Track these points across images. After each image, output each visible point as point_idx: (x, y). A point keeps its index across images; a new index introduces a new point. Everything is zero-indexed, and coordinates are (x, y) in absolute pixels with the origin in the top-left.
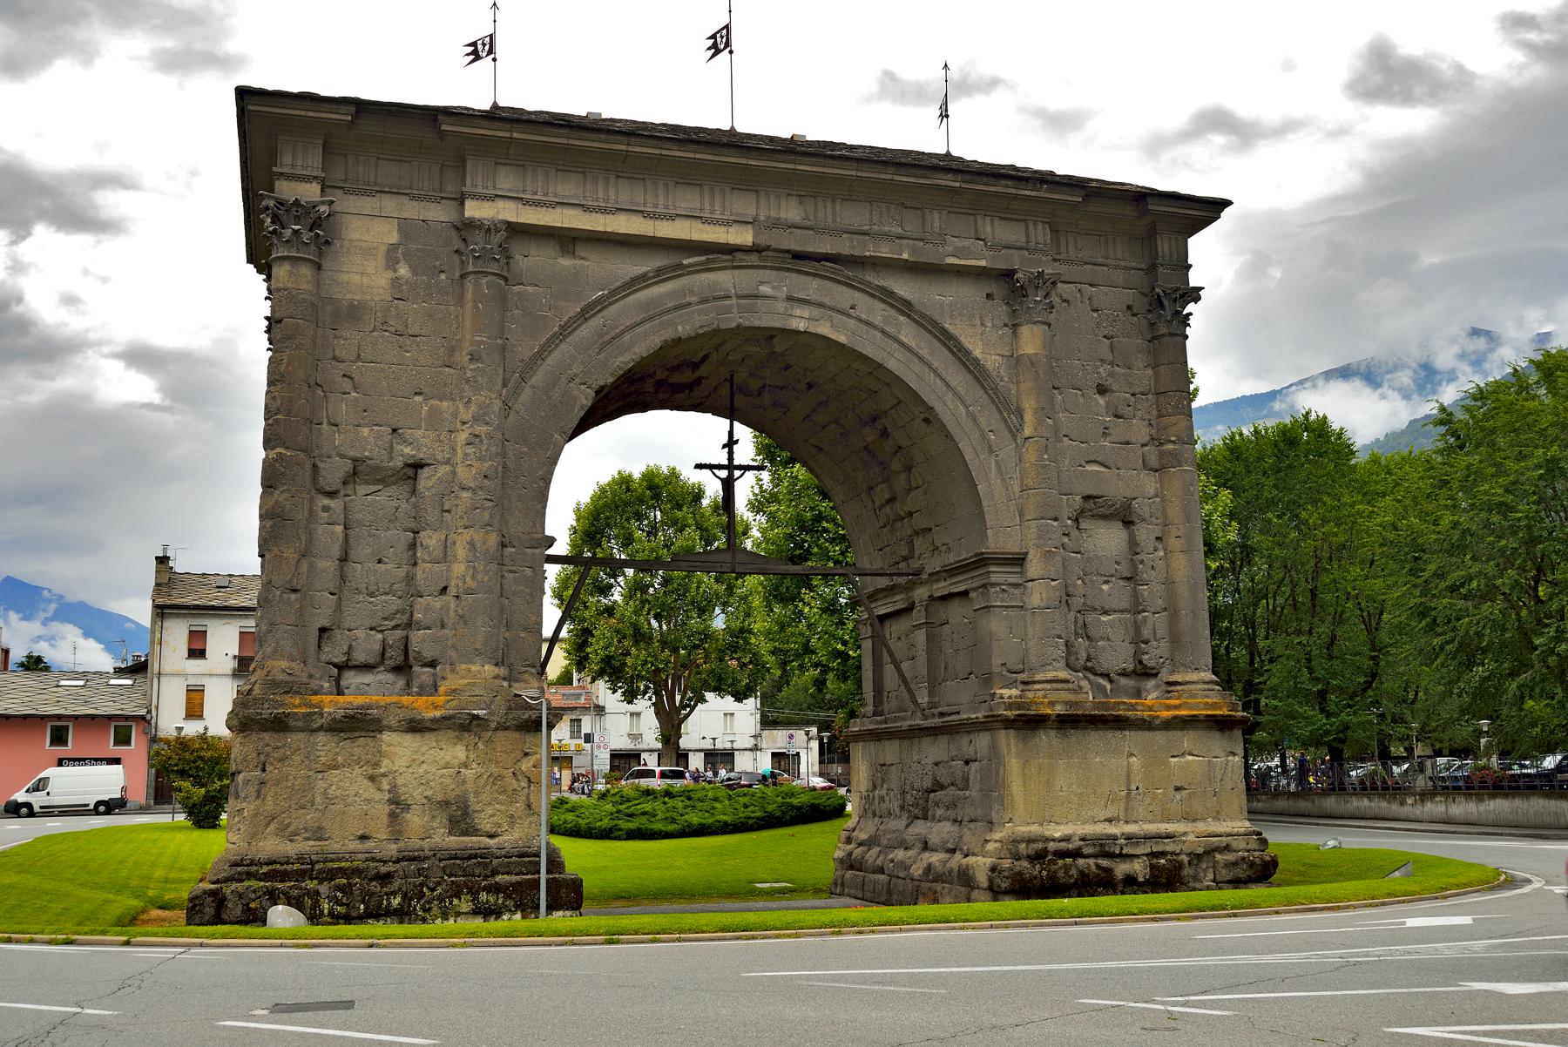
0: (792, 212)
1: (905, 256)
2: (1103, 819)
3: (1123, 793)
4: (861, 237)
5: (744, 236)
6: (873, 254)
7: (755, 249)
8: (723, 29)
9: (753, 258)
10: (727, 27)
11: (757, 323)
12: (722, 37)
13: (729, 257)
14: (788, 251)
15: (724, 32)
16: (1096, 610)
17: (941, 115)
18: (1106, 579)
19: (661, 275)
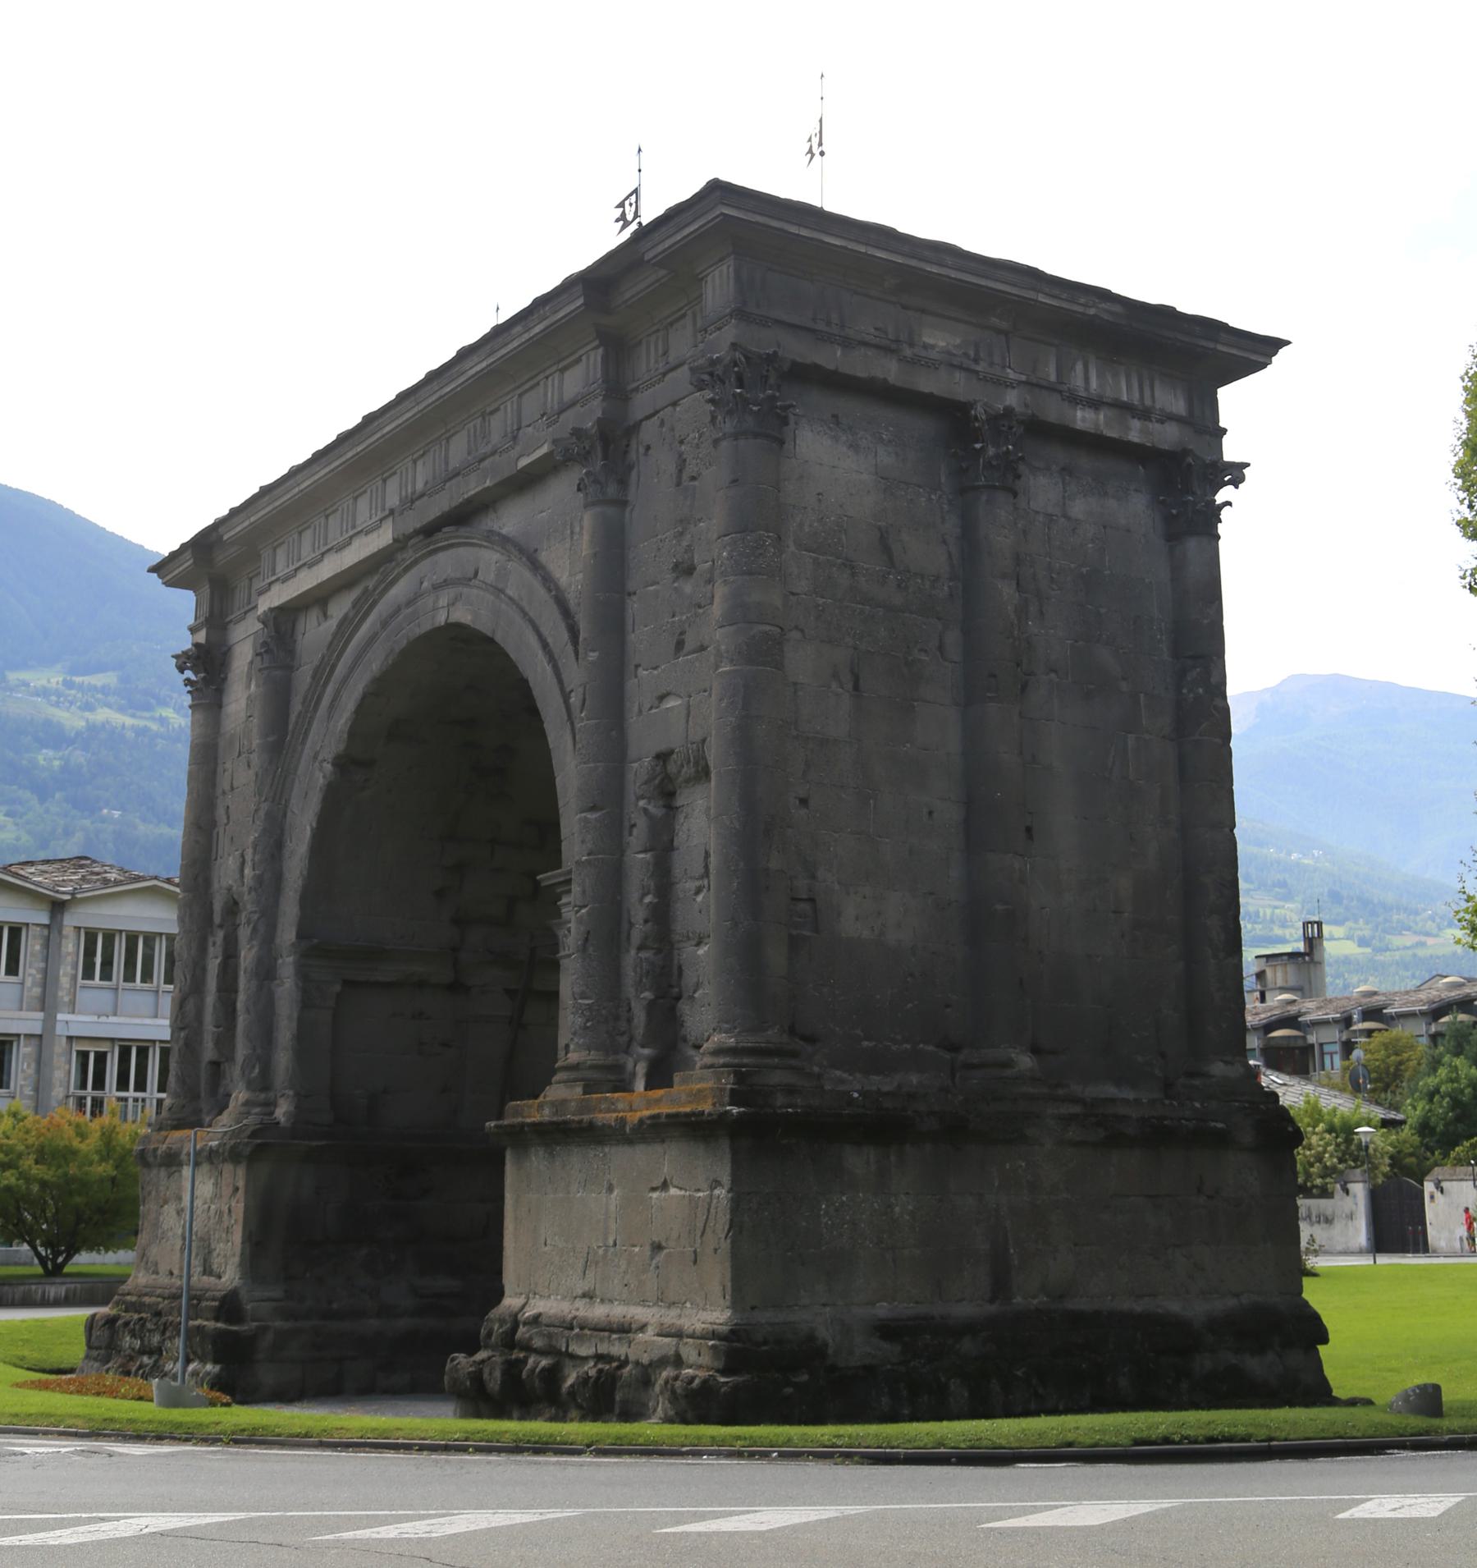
0: (421, 475)
1: (488, 483)
2: (580, 1292)
3: (601, 1252)
4: (454, 481)
5: (383, 538)
6: (466, 496)
7: (400, 543)
8: (631, 195)
9: (409, 555)
10: (636, 191)
11: (419, 631)
12: (631, 205)
13: (394, 563)
14: (417, 532)
15: (633, 198)
16: (689, 938)
17: (810, 151)
18: (698, 883)
19: (362, 608)
